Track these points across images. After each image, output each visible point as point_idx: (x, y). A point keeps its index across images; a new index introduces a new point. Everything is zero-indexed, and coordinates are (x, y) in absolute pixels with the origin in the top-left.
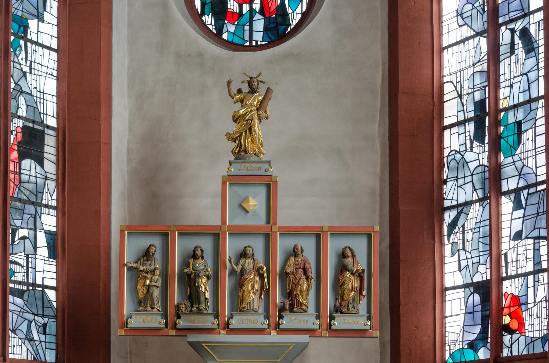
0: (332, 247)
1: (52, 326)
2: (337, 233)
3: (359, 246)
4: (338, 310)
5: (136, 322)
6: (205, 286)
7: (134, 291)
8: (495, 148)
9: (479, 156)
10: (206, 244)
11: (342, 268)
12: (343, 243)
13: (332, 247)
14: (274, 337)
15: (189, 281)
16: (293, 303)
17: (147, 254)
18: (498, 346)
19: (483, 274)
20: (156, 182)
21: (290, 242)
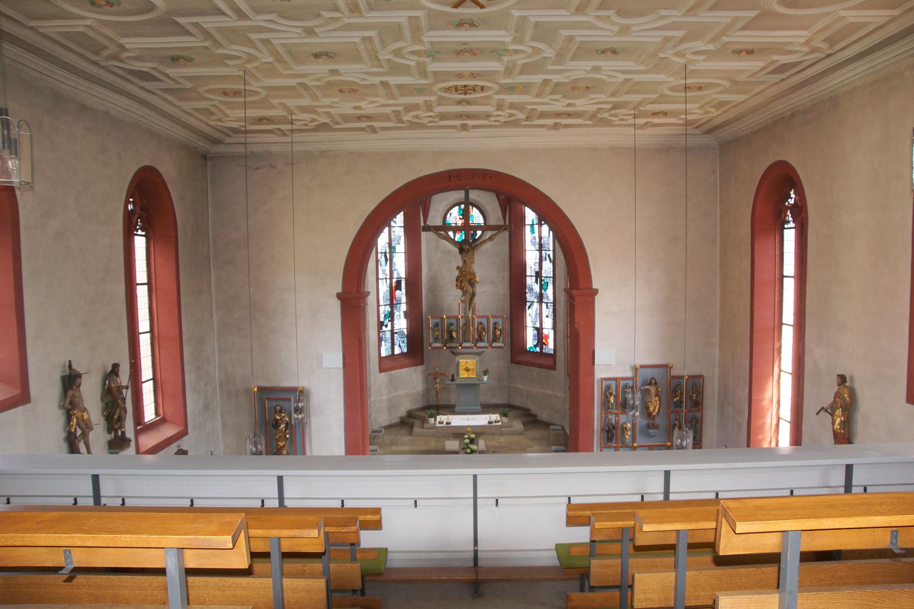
0: (492, 321)
1: (405, 340)
2: (493, 317)
3: (500, 321)
4: (494, 341)
5: (435, 345)
6: (454, 334)
7: (433, 335)
8: (541, 288)
9: (536, 288)
10: (454, 321)
11: (495, 328)
12: (495, 320)
13: (492, 321)
14: (475, 350)
15: (450, 333)
16: (480, 339)
17: (437, 325)
18: (541, 349)
19: (538, 325)
20: (434, 288)
21: (480, 320)
